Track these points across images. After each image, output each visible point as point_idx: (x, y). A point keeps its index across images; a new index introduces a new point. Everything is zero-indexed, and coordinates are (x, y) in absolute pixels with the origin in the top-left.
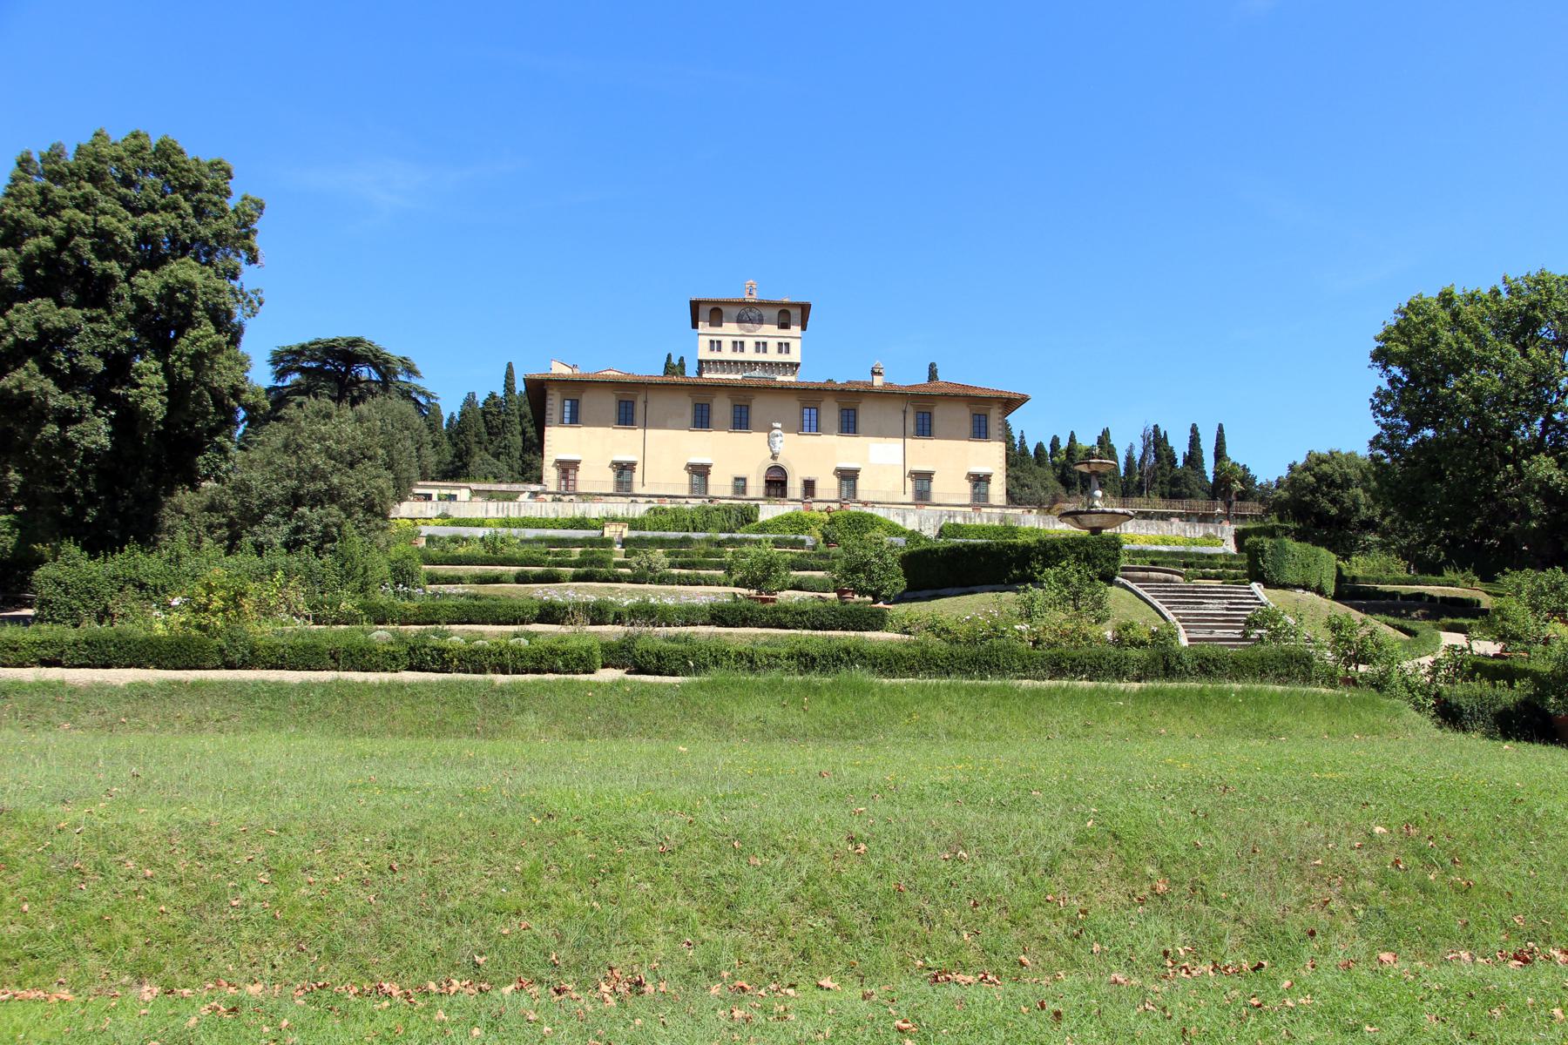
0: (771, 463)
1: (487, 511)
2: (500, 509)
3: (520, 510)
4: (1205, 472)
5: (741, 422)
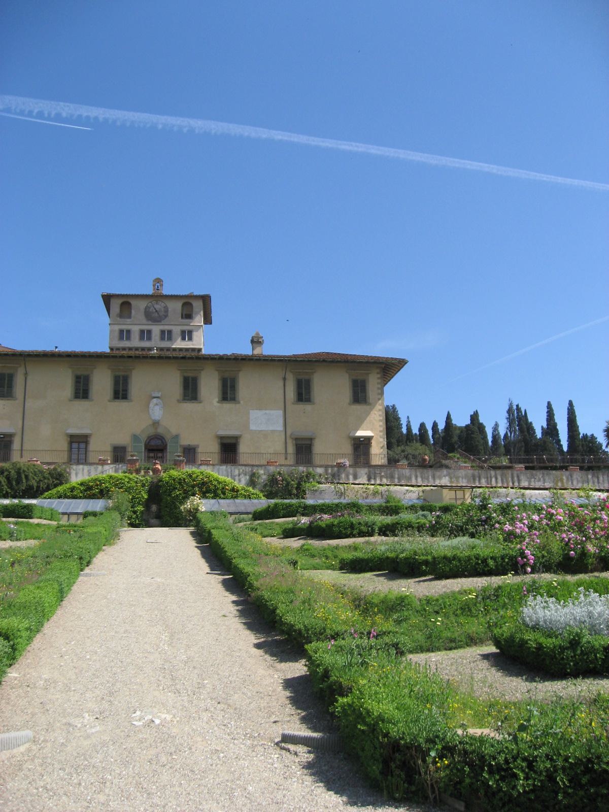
0: (151, 432)
4: (559, 441)
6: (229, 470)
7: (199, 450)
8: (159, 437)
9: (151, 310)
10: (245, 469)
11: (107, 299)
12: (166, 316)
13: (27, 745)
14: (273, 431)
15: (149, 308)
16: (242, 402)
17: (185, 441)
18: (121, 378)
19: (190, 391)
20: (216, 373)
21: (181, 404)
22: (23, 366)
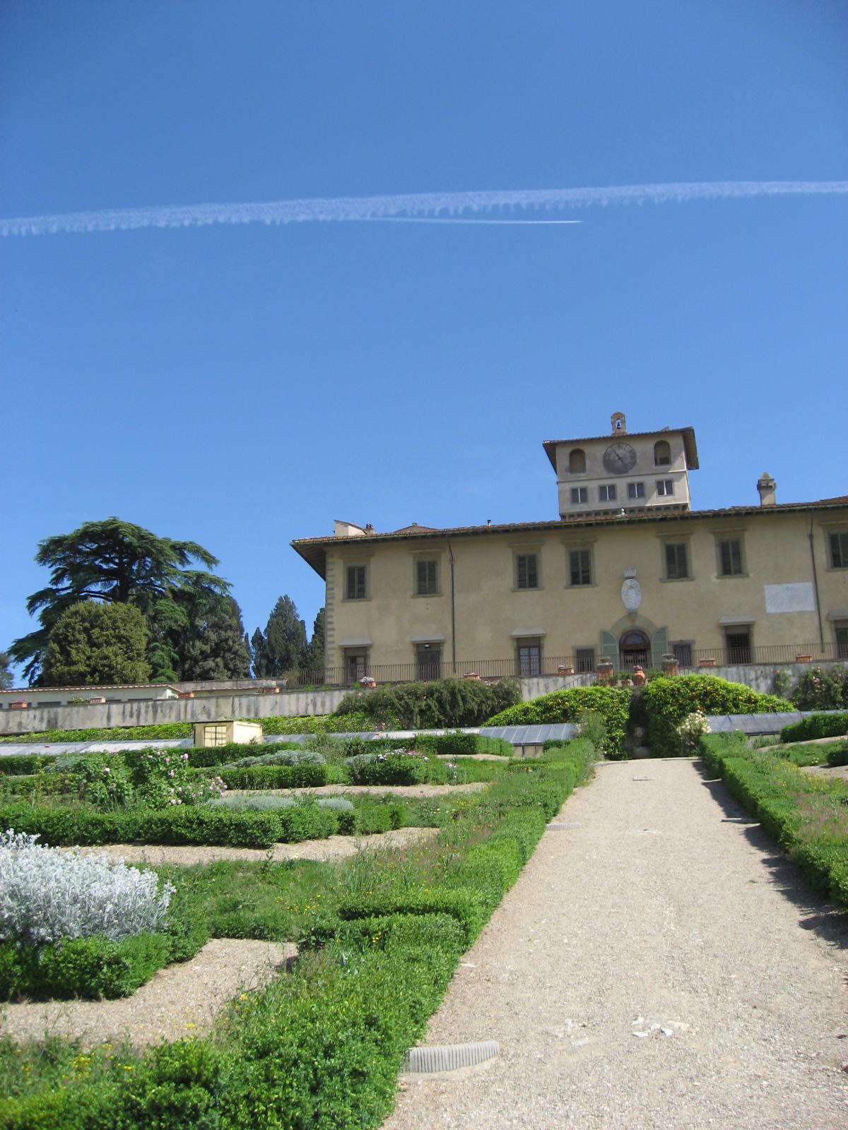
0: (627, 625)
1: (109, 718)
2: (127, 713)
3: (155, 712)
5: (580, 574)
6: (742, 673)
7: (697, 647)
8: (638, 633)
9: (612, 458)
10: (765, 670)
11: (551, 449)
12: (634, 464)
13: (493, 1060)
14: (802, 613)
15: (610, 454)
16: (751, 575)
17: (675, 636)
18: (580, 556)
19: (677, 564)
20: (712, 537)
21: (665, 585)
22: (447, 552)
